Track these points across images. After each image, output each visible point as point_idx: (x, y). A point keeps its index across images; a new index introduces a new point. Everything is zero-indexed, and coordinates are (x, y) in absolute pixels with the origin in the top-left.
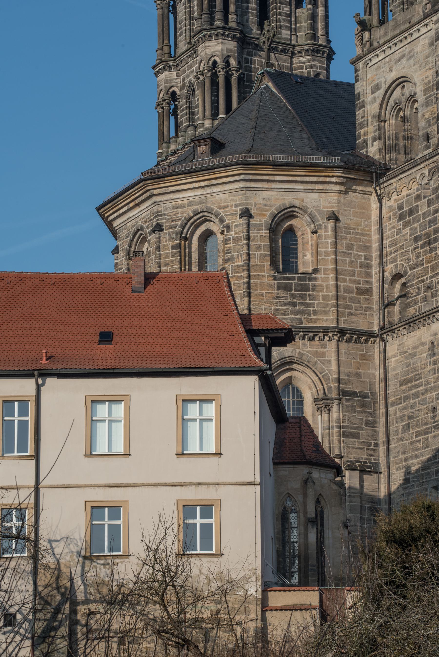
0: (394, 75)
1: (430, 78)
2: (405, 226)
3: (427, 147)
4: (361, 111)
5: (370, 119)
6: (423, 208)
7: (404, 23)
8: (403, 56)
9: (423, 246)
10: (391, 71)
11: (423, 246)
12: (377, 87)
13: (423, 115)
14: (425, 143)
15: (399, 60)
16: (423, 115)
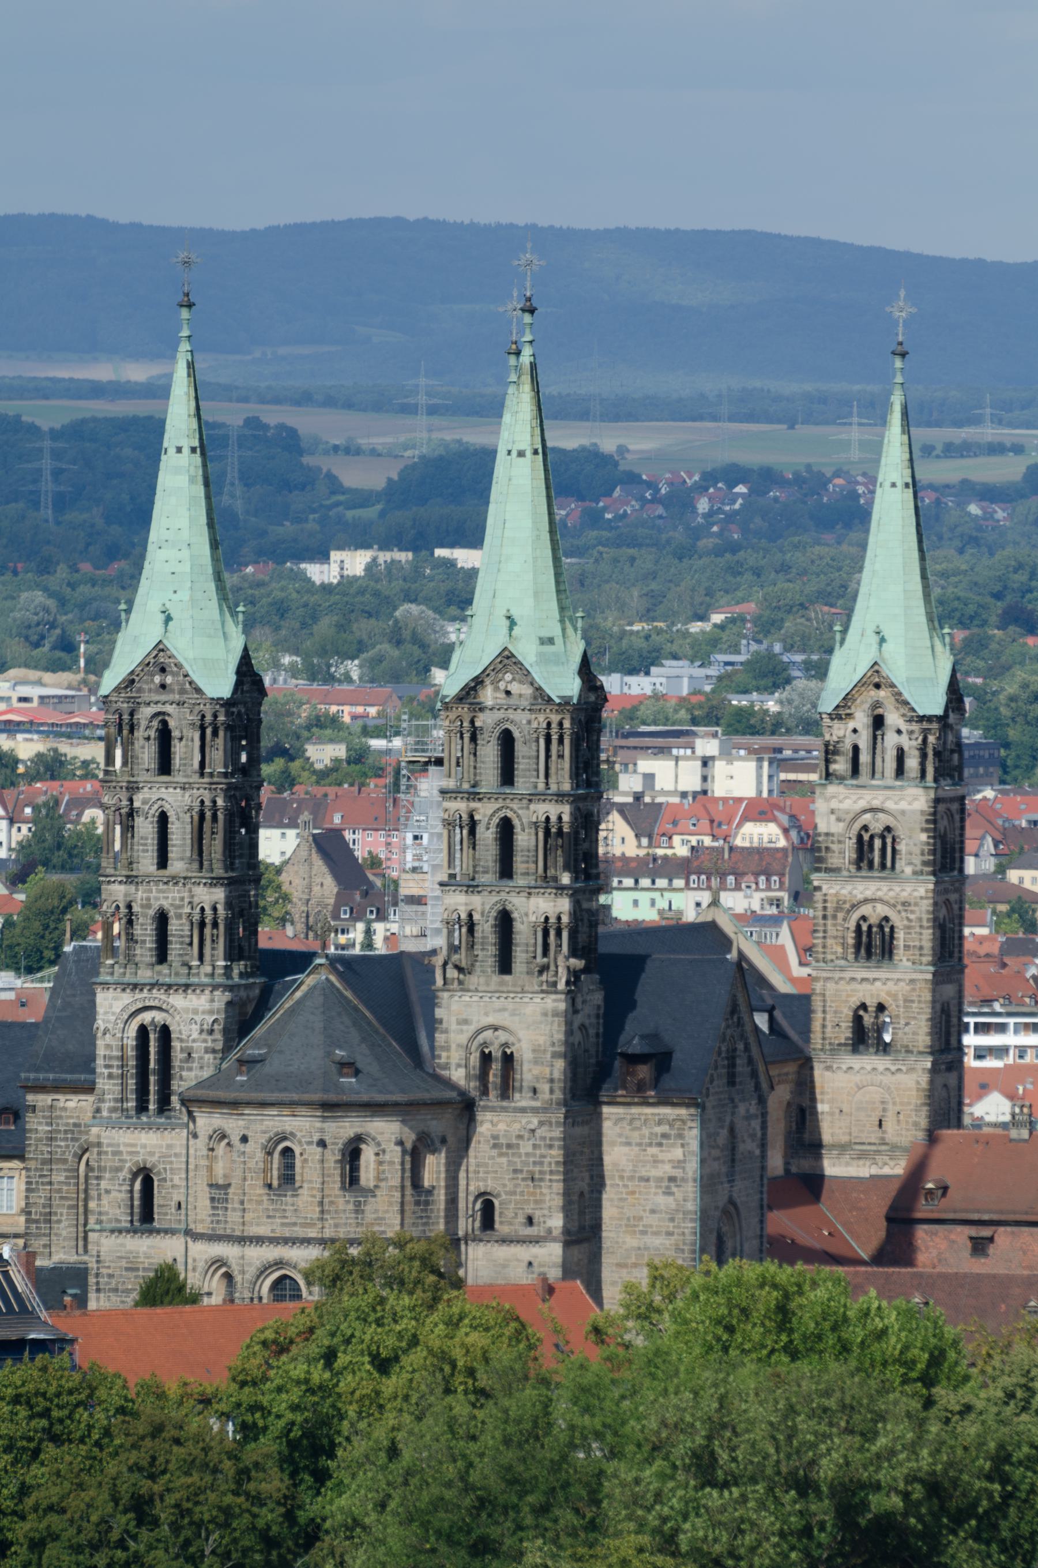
0: (490, 1020)
1: (541, 1042)
2: (501, 1155)
3: (537, 1099)
4: (443, 1036)
5: (453, 1046)
6: (526, 1147)
7: (514, 985)
8: (504, 1010)
9: (523, 1179)
10: (486, 1014)
11: (523, 1179)
12: (466, 1022)
13: (530, 1070)
14: (531, 1094)
15: (500, 1010)
16: (530, 1070)
